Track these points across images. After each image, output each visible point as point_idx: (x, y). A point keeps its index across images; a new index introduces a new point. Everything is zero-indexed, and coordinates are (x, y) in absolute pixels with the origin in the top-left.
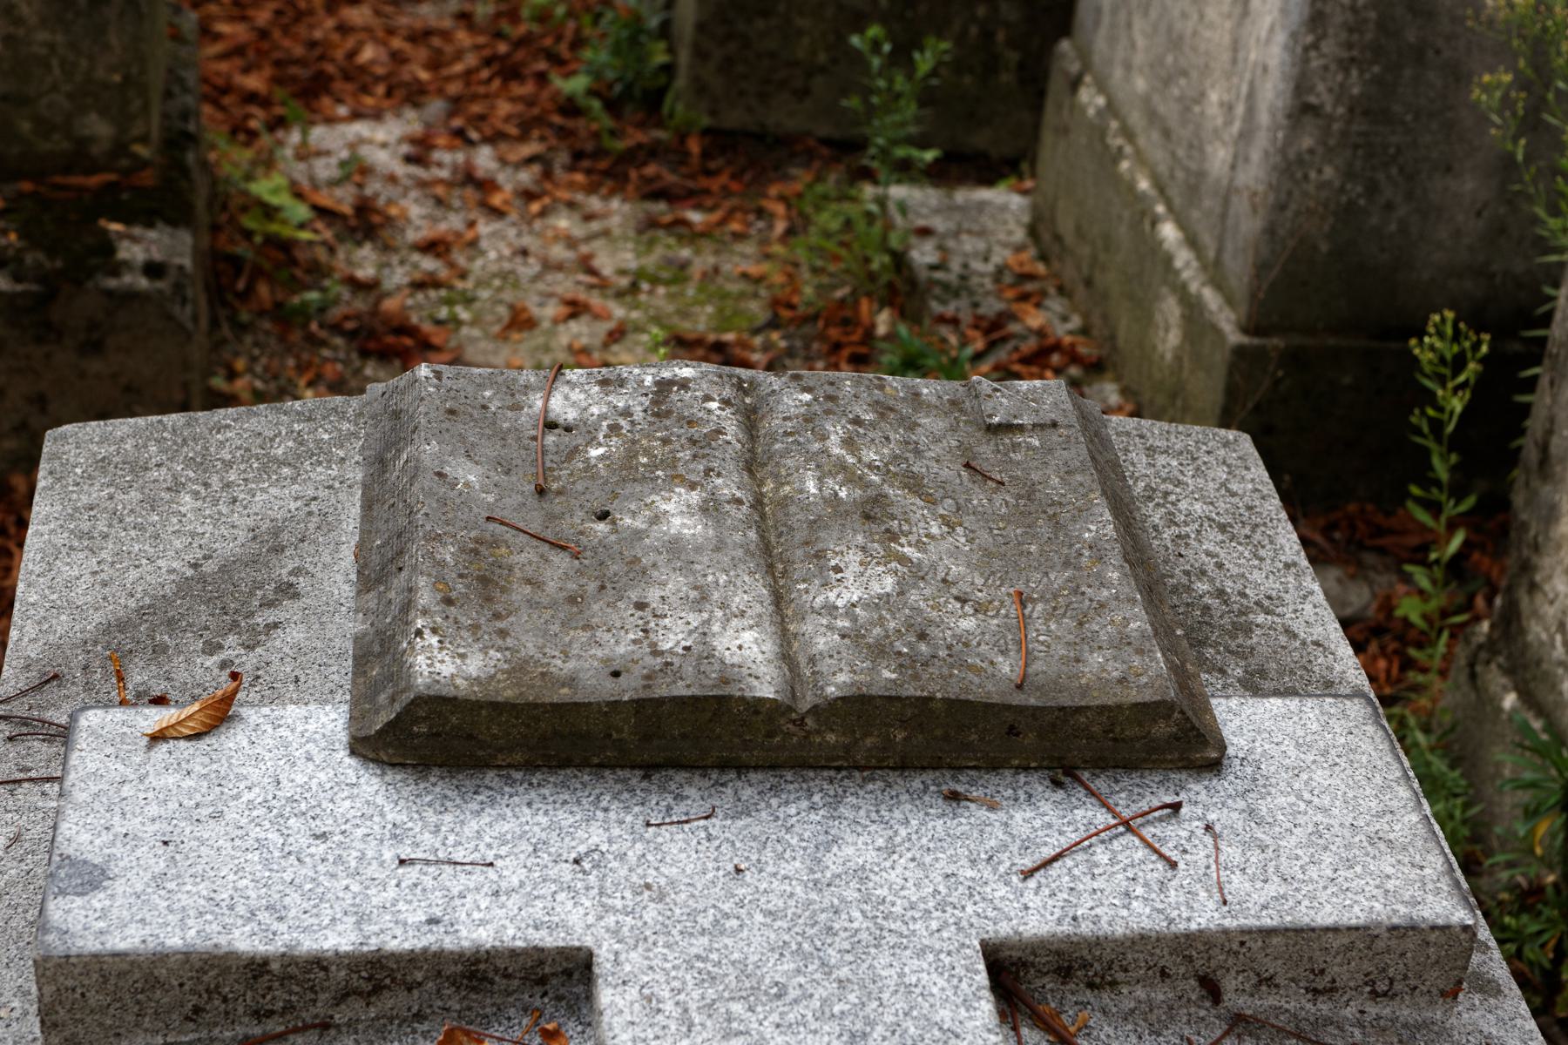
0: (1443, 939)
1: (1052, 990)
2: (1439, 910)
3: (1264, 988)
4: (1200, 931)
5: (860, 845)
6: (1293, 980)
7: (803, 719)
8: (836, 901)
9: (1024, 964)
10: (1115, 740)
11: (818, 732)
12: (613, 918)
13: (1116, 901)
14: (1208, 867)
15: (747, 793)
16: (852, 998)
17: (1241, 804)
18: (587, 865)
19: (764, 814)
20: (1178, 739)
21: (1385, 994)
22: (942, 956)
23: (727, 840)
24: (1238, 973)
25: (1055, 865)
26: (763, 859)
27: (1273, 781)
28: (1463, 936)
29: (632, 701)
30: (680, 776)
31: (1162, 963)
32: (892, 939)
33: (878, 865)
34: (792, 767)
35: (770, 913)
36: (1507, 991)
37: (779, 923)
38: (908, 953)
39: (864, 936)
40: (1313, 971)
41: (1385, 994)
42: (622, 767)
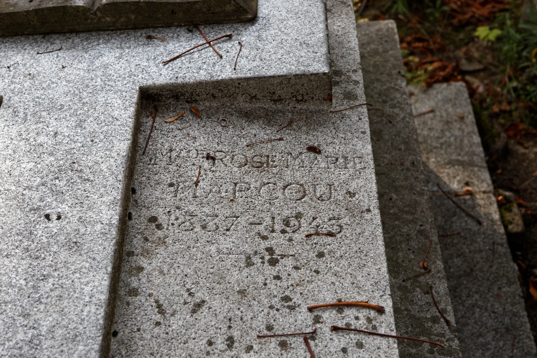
0: (317, 79)
1: (173, 104)
2: (316, 68)
3: (254, 100)
4: (222, 80)
5: (110, 56)
6: (264, 96)
7: (95, 13)
8: (93, 76)
9: (160, 95)
10: (213, 13)
11: (103, 17)
12: (14, 86)
13: (195, 71)
14: (234, 57)
15: (77, 40)
16: (86, 109)
17: (257, 34)
18: (11, 68)
19: (80, 48)
20: (236, 11)
21: (302, 101)
22: (123, 93)
23: (63, 57)
24: (242, 95)
25: (178, 59)
26: (74, 63)
27: (272, 25)
28: (324, 77)
29: (33, 10)
30: (55, 36)
31: (211, 92)
32: (108, 88)
33: (113, 63)
34: (96, 31)
35: (69, 81)
36: (359, 98)
37: (70, 84)
38: (112, 92)
39: (99, 87)
40: (270, 93)
41: (302, 101)
42: (36, 34)
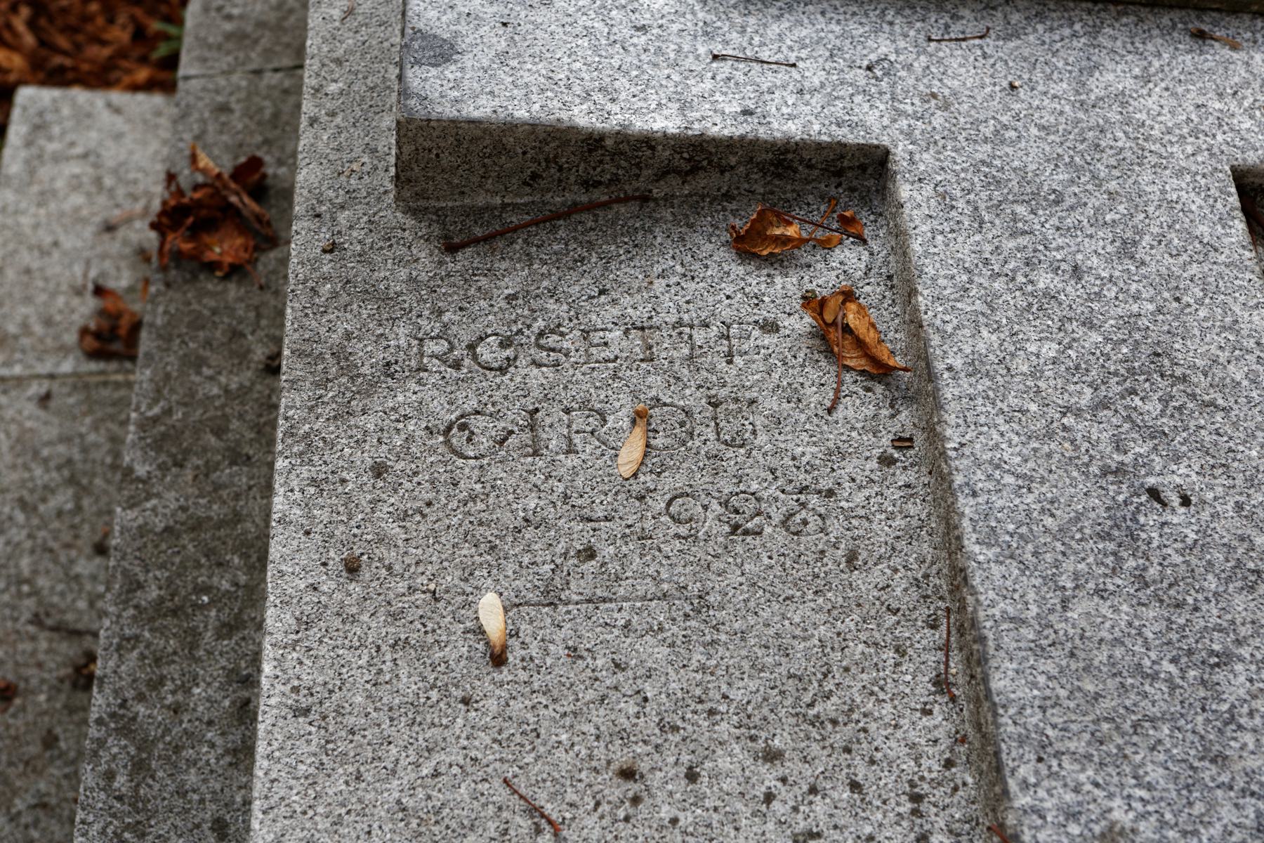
5: (1119, 73)
8: (1101, 121)
15: (1015, 17)
16: (1121, 208)
19: (1031, 38)
22: (1198, 178)
26: (1034, 79)
37: (1052, 137)
38: (1167, 172)
39: (1128, 154)
